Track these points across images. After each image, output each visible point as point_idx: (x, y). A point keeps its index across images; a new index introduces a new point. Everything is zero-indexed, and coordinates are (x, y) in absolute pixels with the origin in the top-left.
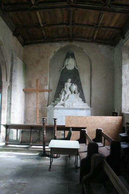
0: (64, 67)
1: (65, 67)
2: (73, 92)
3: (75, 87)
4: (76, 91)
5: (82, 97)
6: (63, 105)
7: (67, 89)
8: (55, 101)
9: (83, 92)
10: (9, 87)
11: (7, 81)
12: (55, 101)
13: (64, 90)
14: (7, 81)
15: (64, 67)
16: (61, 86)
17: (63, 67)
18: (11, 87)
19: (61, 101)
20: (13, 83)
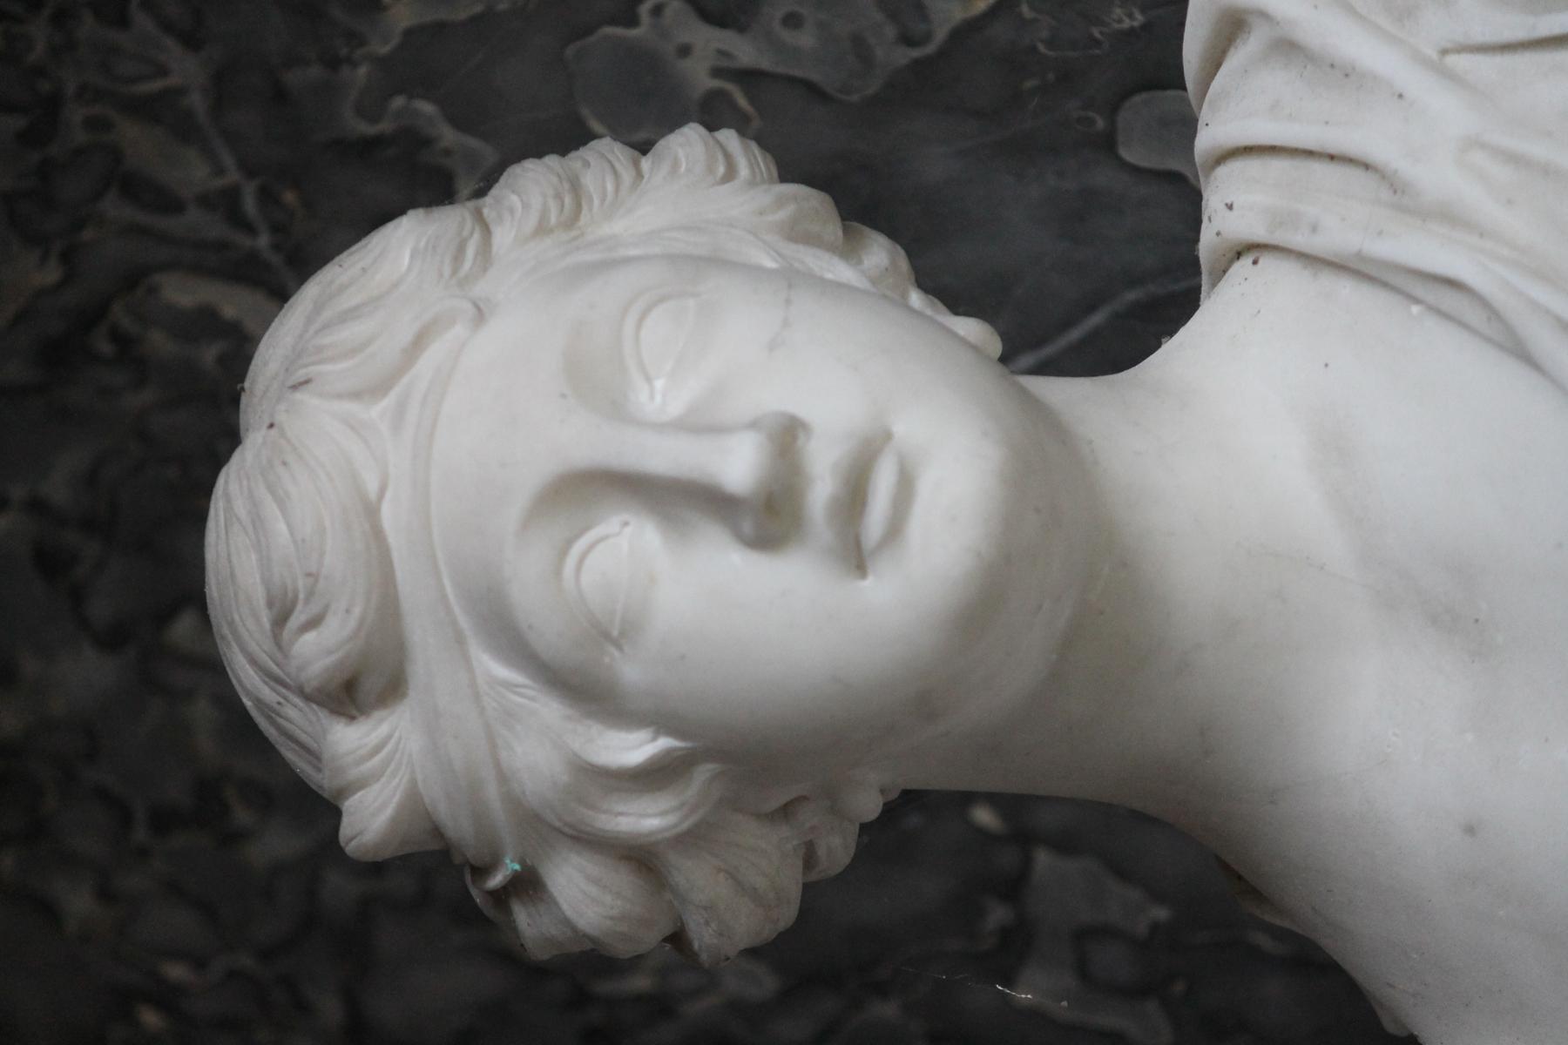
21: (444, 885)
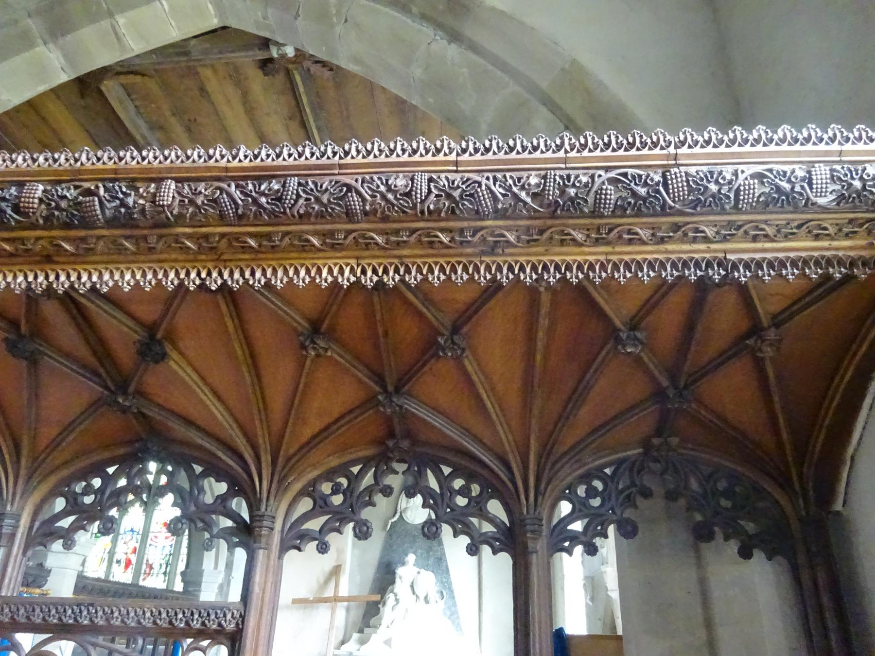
0: (395, 519)
1: (401, 516)
2: (422, 598)
3: (427, 580)
4: (434, 596)
5: (451, 615)
6: (388, 642)
7: (401, 586)
8: (366, 630)
9: (453, 598)
10: (221, 587)
11: (216, 567)
12: (366, 630)
13: (392, 591)
14: (216, 567)
15: (395, 519)
16: (385, 578)
17: (394, 516)
18: (229, 585)
19: (382, 629)
20: (233, 575)
21: (407, 555)
